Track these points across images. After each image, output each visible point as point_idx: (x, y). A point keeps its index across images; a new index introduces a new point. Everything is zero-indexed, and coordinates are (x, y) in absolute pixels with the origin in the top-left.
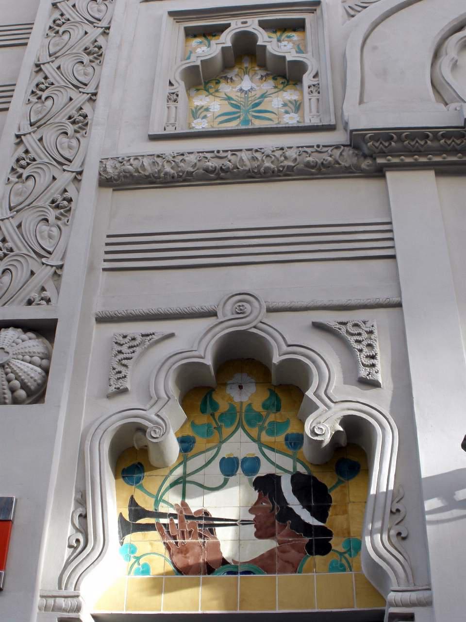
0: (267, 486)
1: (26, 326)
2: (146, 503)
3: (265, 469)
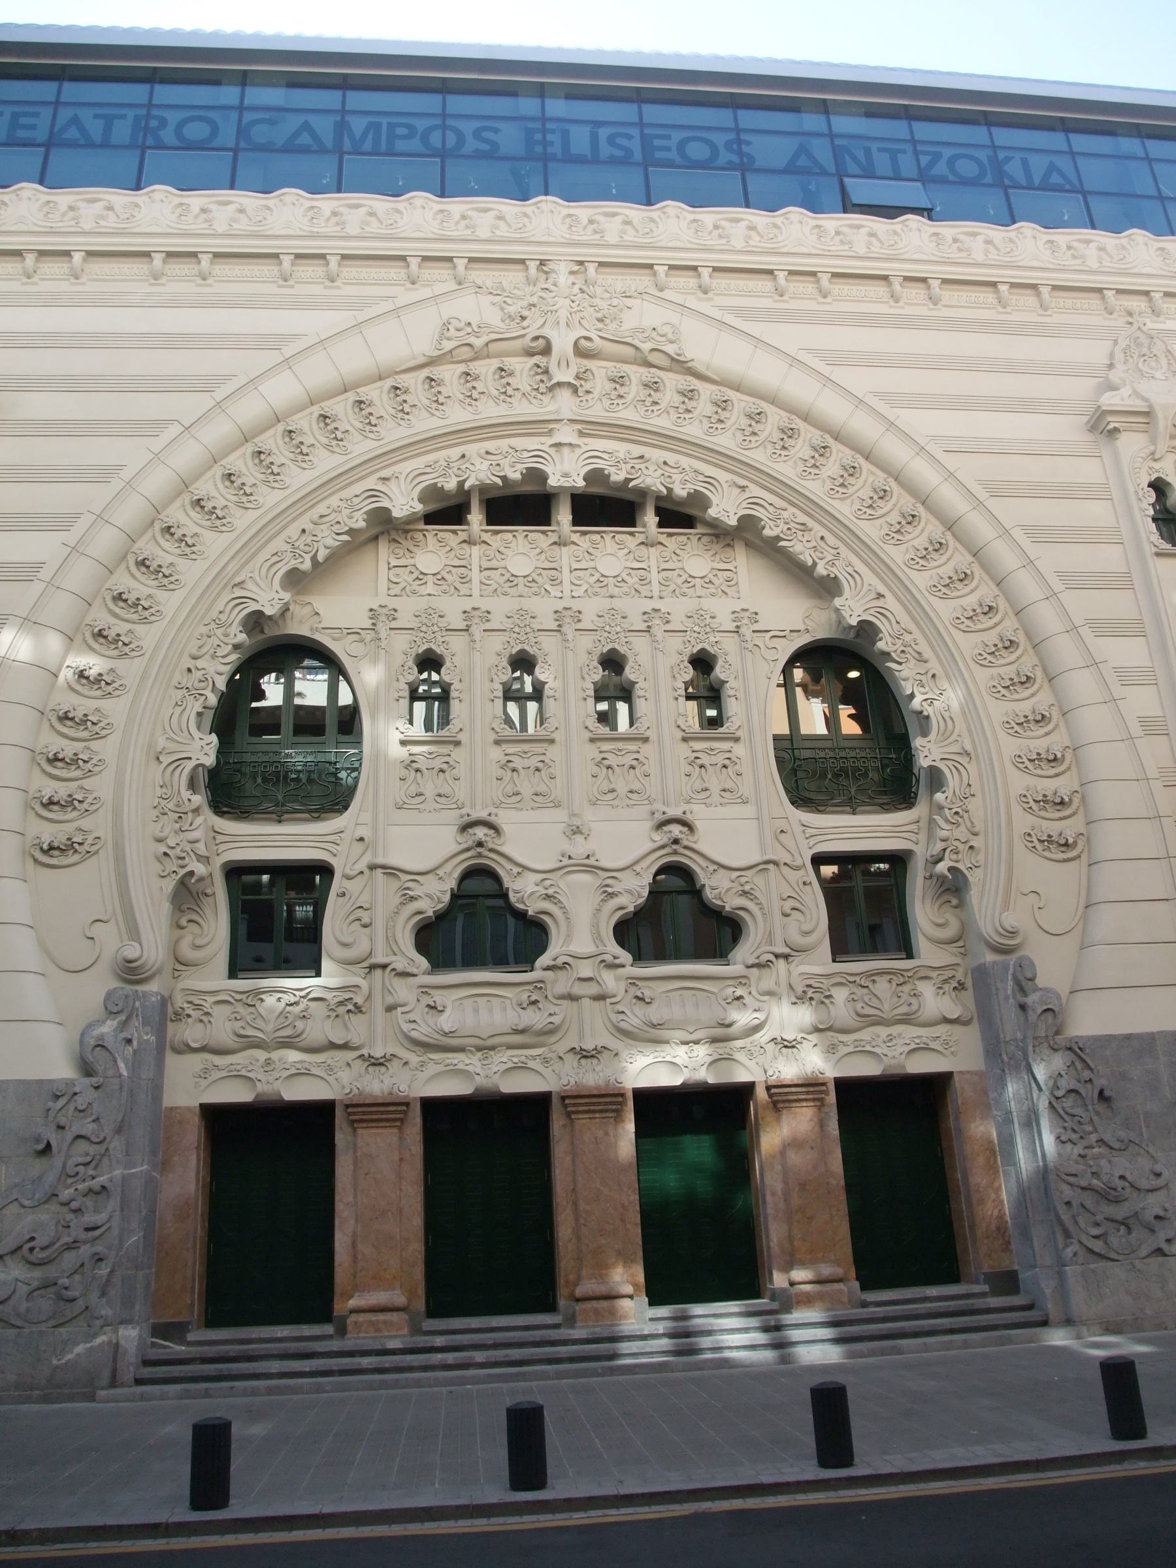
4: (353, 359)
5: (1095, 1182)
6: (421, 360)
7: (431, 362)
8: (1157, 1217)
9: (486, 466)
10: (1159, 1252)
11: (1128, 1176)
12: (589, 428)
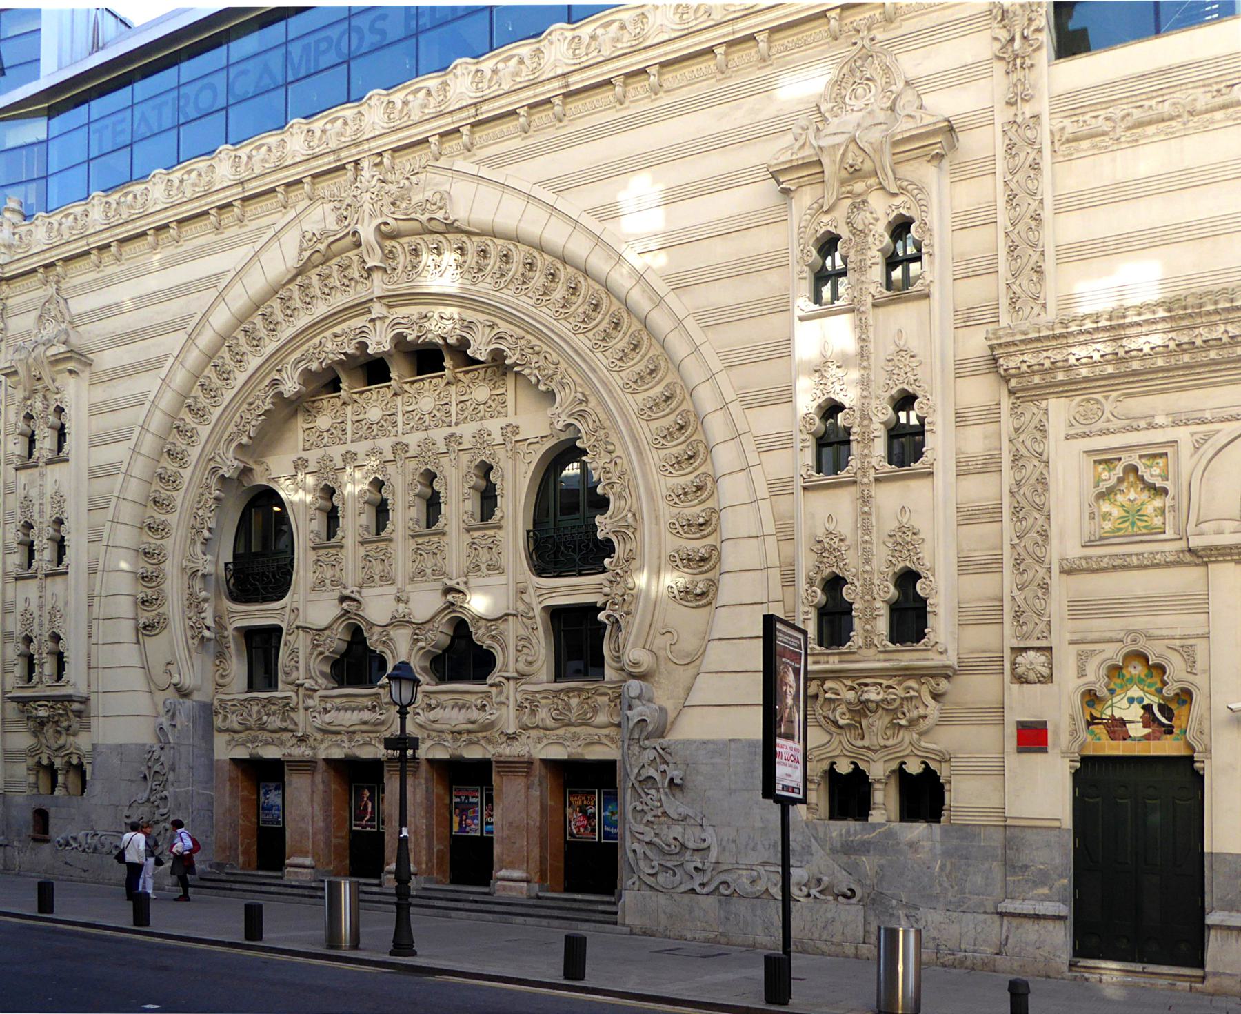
0: (1148, 708)
1: (1038, 649)
2: (1097, 714)
3: (1146, 702)
4: (256, 283)
5: (656, 840)
6: (294, 272)
7: (300, 272)
8: (696, 868)
9: (333, 347)
10: (693, 891)
11: (680, 838)
12: (392, 300)
